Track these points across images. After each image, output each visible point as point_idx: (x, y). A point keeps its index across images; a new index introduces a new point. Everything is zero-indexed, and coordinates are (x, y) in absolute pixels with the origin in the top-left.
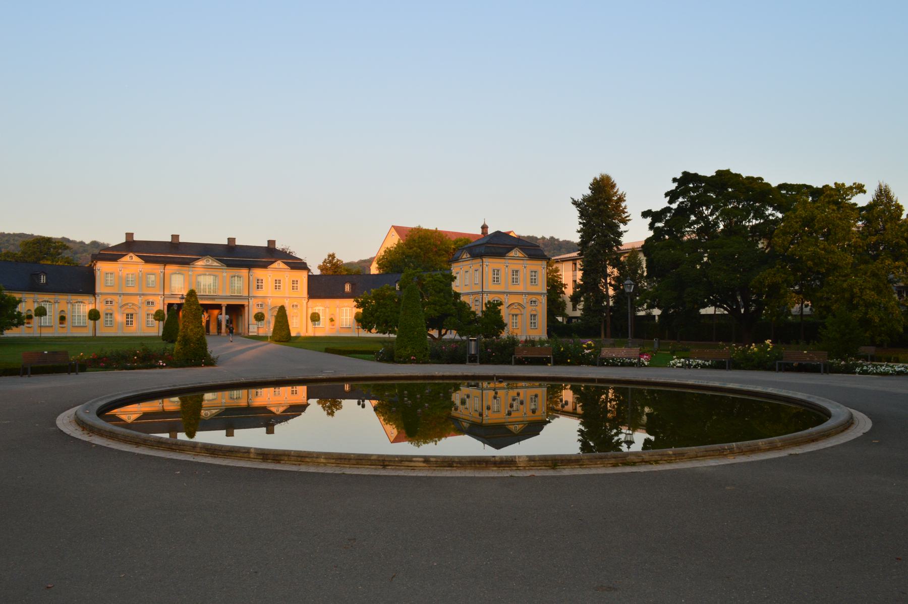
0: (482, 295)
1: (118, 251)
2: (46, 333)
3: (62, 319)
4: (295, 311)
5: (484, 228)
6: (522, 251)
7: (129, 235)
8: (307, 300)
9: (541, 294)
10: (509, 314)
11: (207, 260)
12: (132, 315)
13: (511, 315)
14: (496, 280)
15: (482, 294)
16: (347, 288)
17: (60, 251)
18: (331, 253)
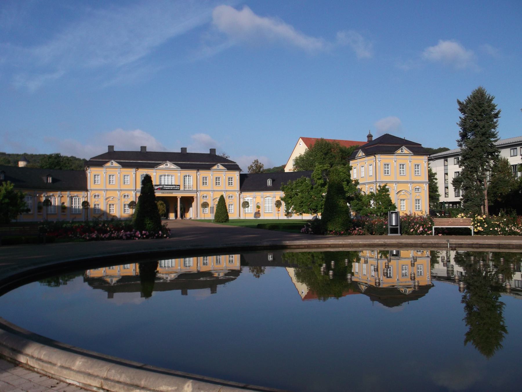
0: (376, 184)
1: (103, 159)
4: (231, 201)
5: (370, 136)
7: (111, 147)
10: (398, 199)
11: (166, 164)
13: (399, 200)
14: (386, 172)
15: (376, 183)
16: (269, 182)
18: (256, 159)
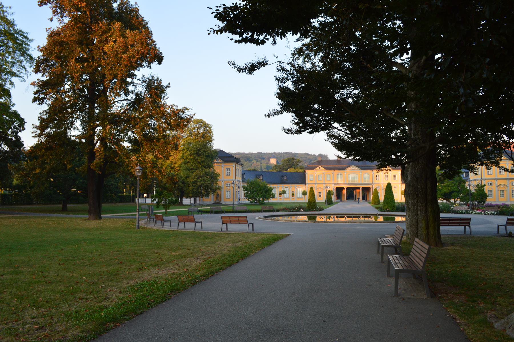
1: (315, 165)
2: (286, 201)
3: (293, 195)
4: (395, 190)
8: (401, 184)
12: (321, 193)
17: (298, 163)
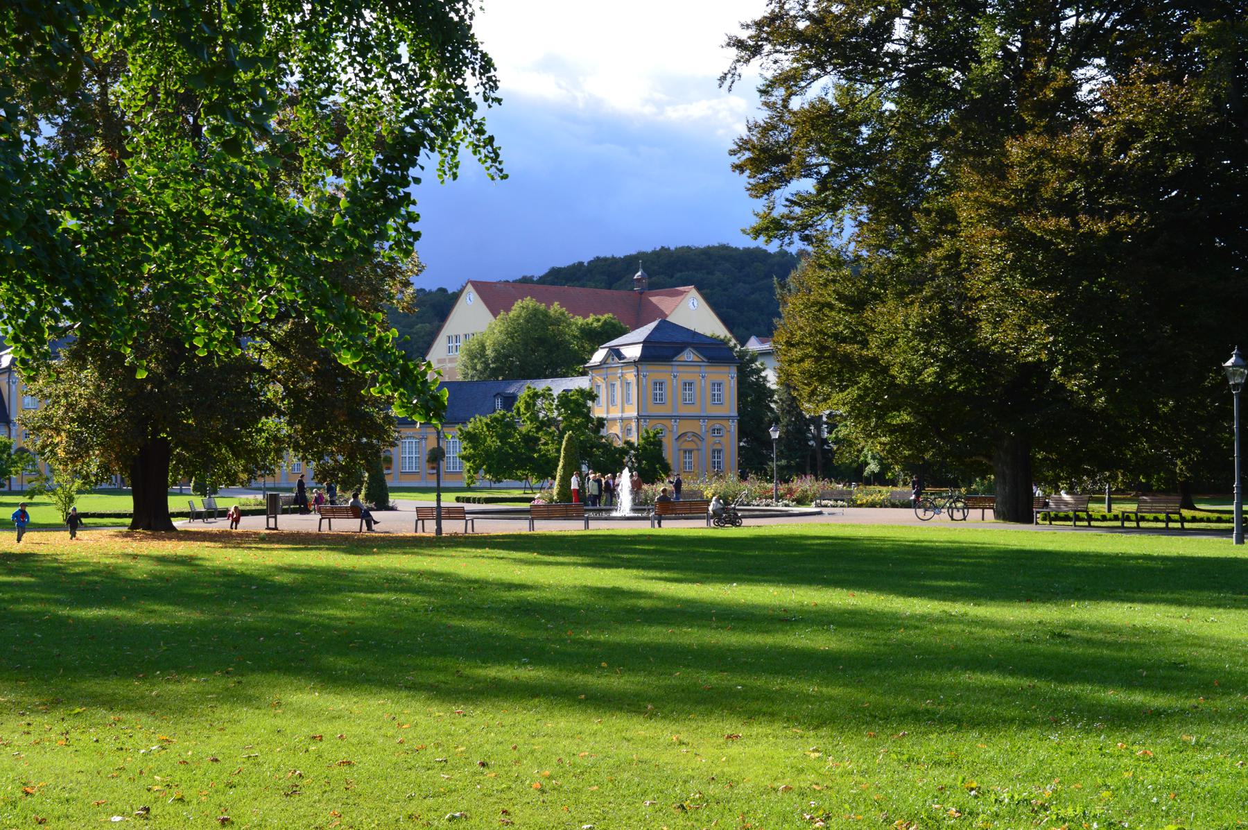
6: (699, 352)
9: (728, 418)
